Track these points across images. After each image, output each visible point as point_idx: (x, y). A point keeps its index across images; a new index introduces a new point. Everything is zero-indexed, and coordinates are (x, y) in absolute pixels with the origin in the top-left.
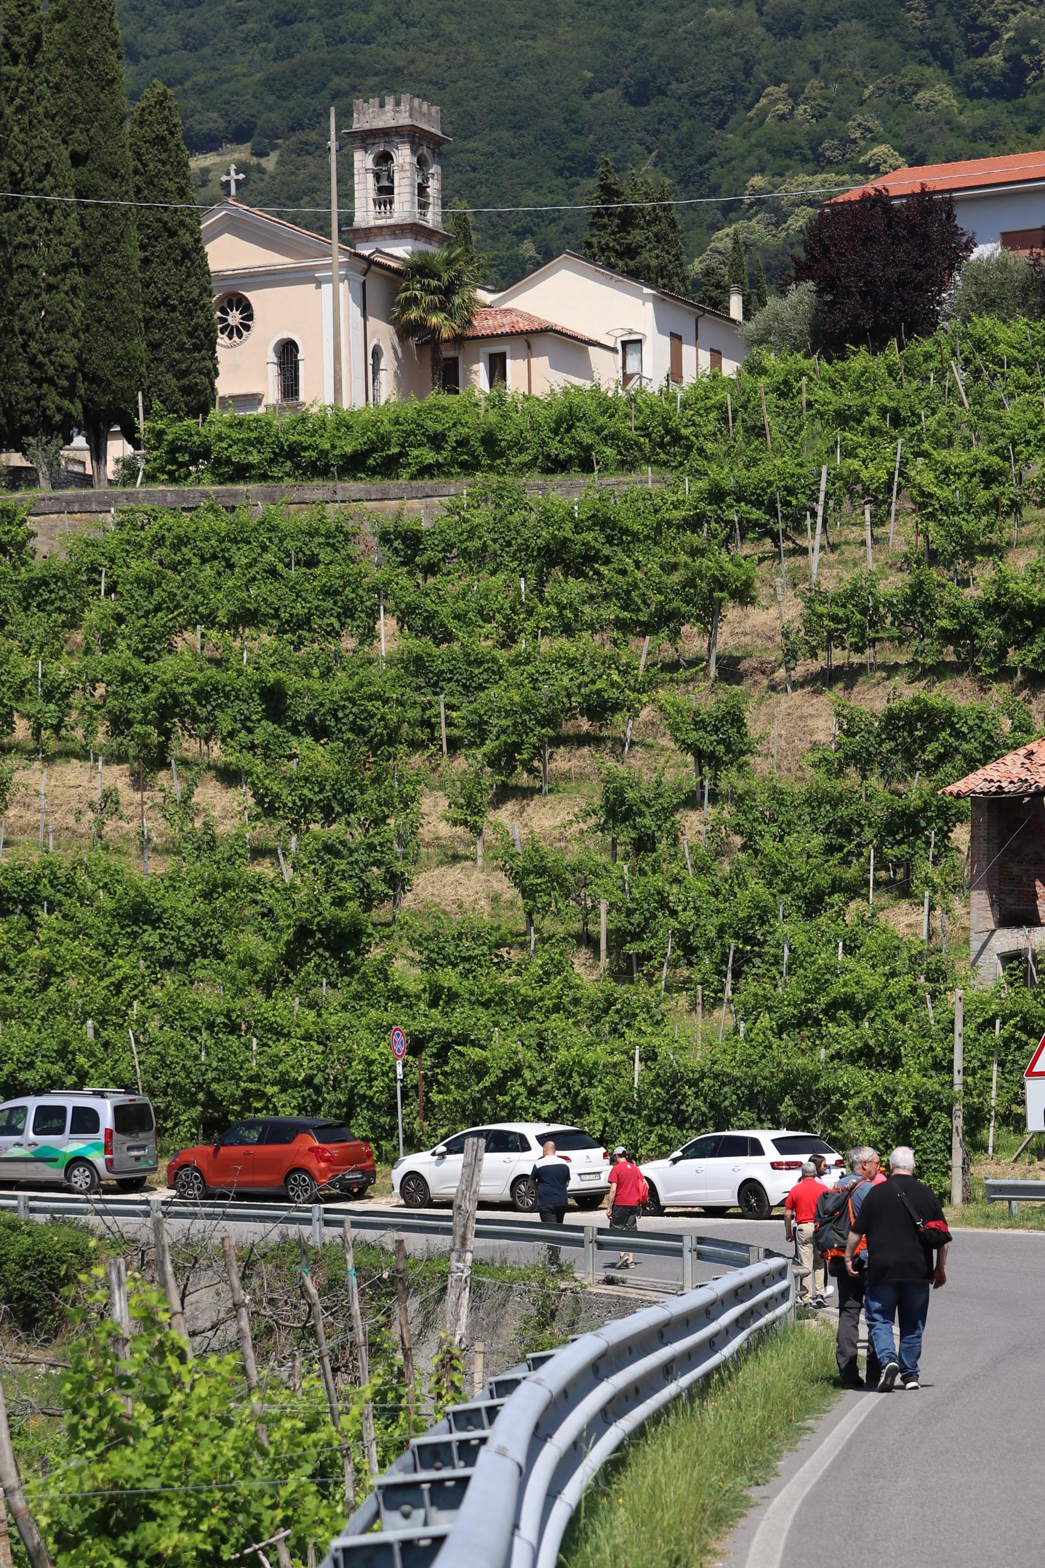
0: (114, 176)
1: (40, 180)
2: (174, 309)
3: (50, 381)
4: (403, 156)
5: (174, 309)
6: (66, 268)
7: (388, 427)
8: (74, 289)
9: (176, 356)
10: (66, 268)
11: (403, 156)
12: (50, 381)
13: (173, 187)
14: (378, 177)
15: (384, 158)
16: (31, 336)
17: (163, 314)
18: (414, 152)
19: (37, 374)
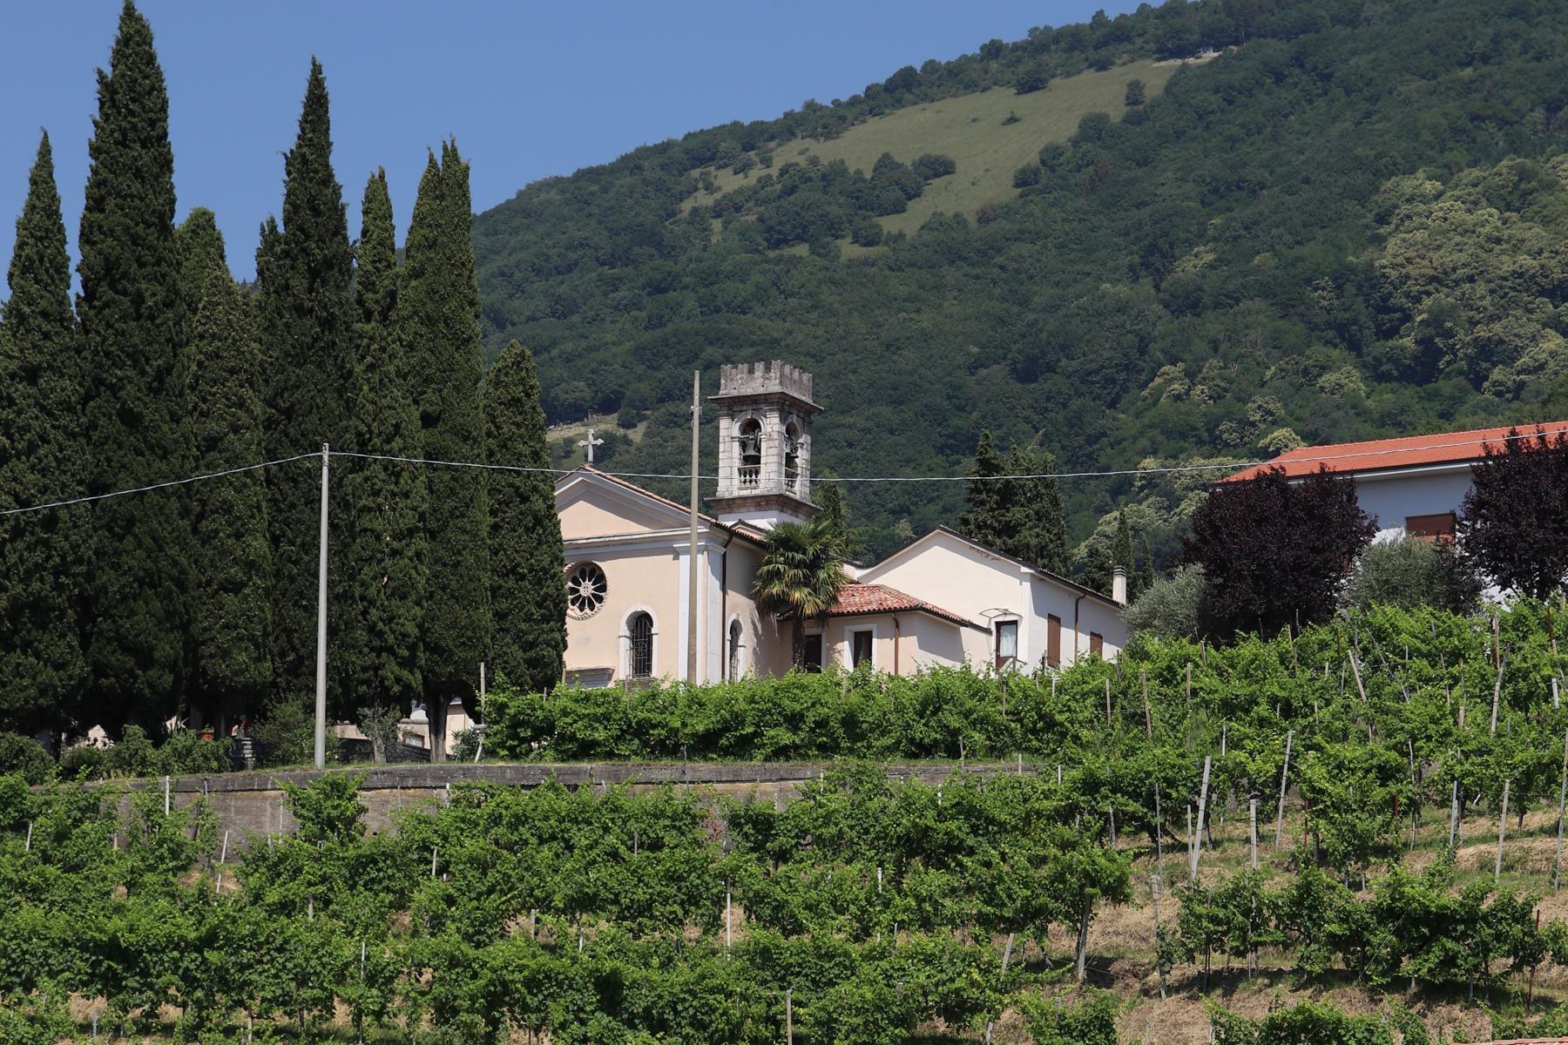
2: (523, 577)
5: (523, 577)
17: (511, 582)
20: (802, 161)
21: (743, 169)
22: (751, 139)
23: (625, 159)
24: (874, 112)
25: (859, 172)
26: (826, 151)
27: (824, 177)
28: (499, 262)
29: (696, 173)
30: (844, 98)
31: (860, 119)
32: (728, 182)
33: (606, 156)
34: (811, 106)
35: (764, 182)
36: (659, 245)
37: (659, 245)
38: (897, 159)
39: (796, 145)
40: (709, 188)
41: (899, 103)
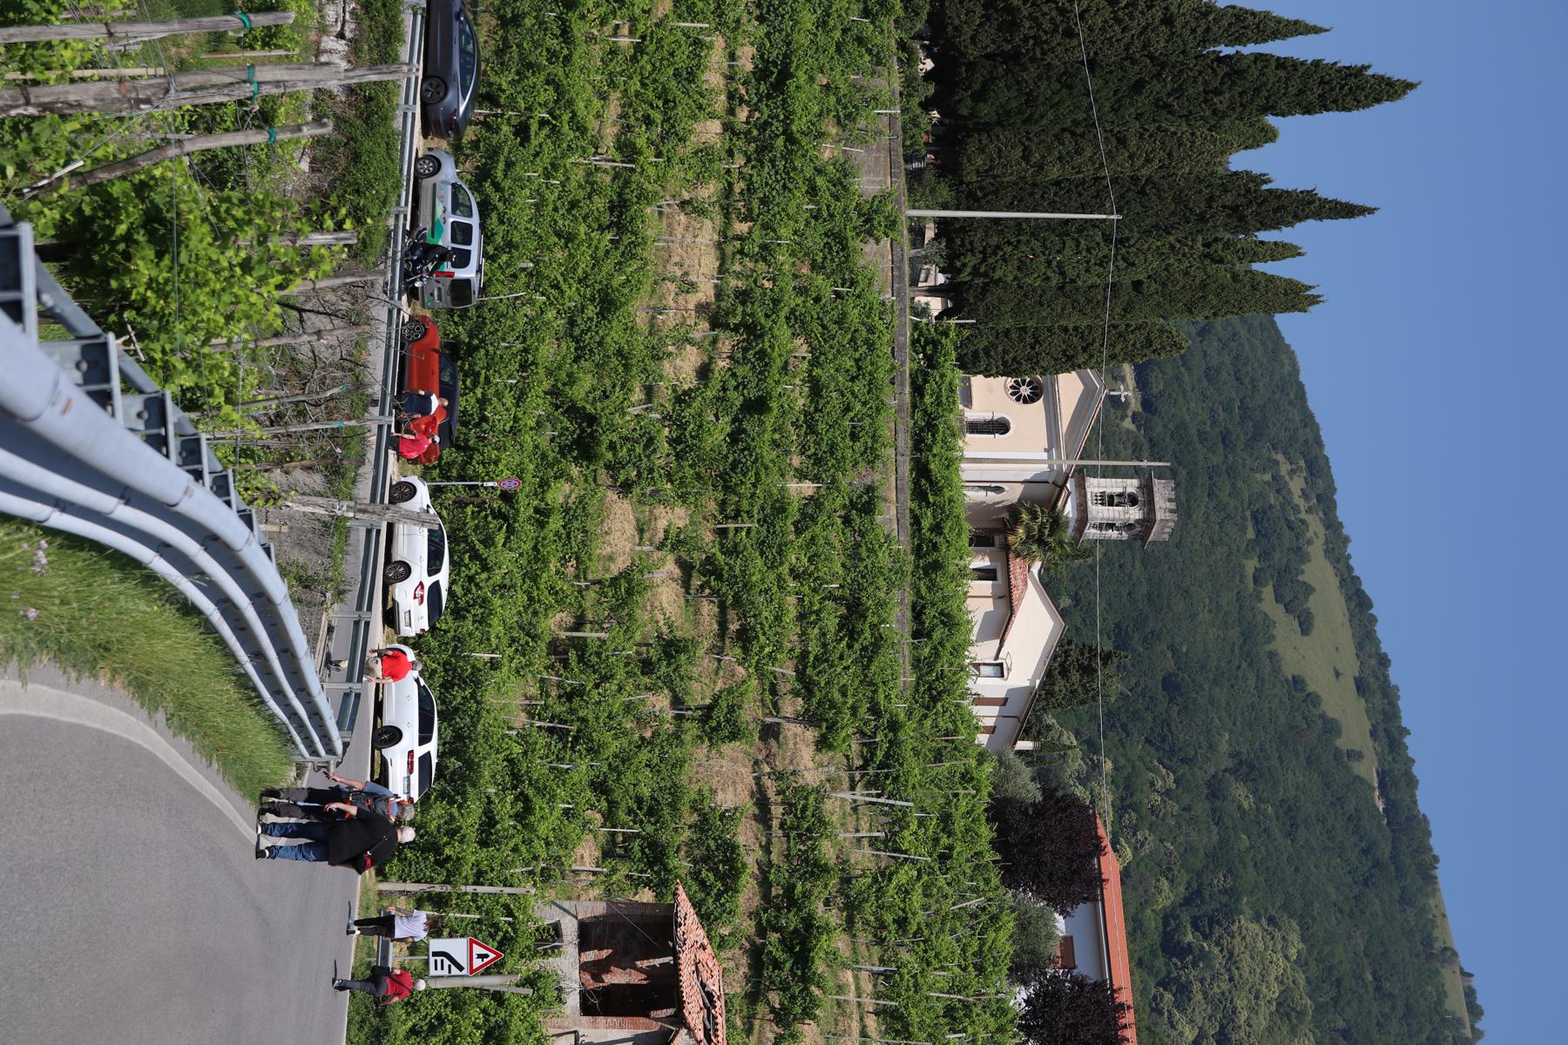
0: (1125, 310)
1: (1124, 259)
2: (1033, 348)
3: (984, 260)
4: (1134, 514)
5: (1033, 348)
6: (1063, 274)
7: (947, 494)
8: (1048, 279)
9: (1000, 349)
10: (1063, 274)
11: (1134, 514)
12: (984, 260)
13: (1117, 350)
14: (1120, 495)
15: (1133, 500)
16: (1016, 248)
17: (1029, 340)
18: (1137, 521)
19: (989, 250)
20: (1309, 534)
21: (1305, 495)
22: (1325, 501)
23: (1311, 416)
24: (1343, 582)
25: (1303, 572)
26: (1316, 550)
27: (1299, 549)
28: (1243, 332)
29: (1302, 463)
30: (1352, 562)
31: (1338, 572)
32: (1296, 485)
33: (1313, 404)
34: (1346, 540)
35: (1296, 509)
36: (1254, 438)
37: (1254, 438)
38: (1311, 598)
39: (1322, 531)
40: (1292, 472)
41: (1348, 599)
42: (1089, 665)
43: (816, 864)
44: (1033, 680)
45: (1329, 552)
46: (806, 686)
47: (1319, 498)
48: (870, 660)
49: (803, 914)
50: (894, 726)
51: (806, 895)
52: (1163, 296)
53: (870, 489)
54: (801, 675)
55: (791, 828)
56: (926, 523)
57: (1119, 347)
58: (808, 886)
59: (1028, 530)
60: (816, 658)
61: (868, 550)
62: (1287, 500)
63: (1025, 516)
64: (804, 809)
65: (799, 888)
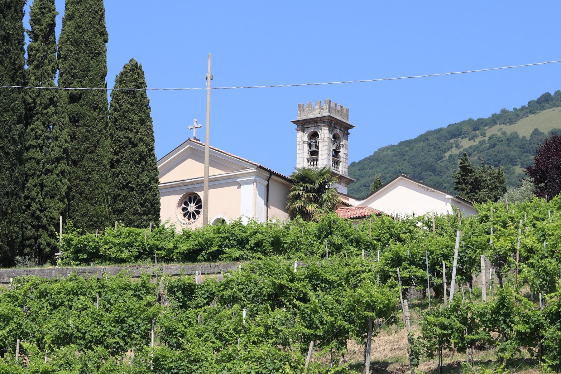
0: (95, 109)
1: (46, 108)
2: (132, 189)
3: (44, 227)
4: (324, 134)
5: (132, 189)
6: (58, 160)
7: (212, 235)
8: (63, 172)
9: (132, 217)
10: (58, 160)
11: (324, 134)
12: (44, 227)
13: (136, 118)
14: (310, 146)
15: (314, 135)
16: (33, 200)
17: (125, 192)
18: (331, 131)
19: (35, 223)
20: (499, 134)
21: (473, 138)
22: (477, 126)
23: (421, 136)
24: (531, 112)
25: (524, 137)
26: (509, 129)
27: (508, 140)
28: (364, 180)
29: (452, 141)
30: (519, 107)
31: (526, 115)
32: (466, 144)
33: (413, 136)
34: (504, 111)
35: (482, 143)
36: (434, 171)
37: (434, 171)
38: (542, 131)
39: (497, 127)
40: (458, 146)
41: (543, 108)
42: (471, 184)
43: (496, 312)
44: (446, 200)
45: (511, 122)
46: (337, 335)
47: (475, 130)
48: (325, 281)
49: (546, 323)
50: (396, 261)
51: (527, 320)
52: (84, 77)
53: (171, 291)
54: (324, 341)
55: (462, 339)
56: (237, 253)
57: (133, 116)
58: (517, 319)
59: (311, 202)
60: (309, 327)
61: (225, 289)
62: (476, 148)
63: (298, 204)
64: (443, 327)
65: (521, 327)
